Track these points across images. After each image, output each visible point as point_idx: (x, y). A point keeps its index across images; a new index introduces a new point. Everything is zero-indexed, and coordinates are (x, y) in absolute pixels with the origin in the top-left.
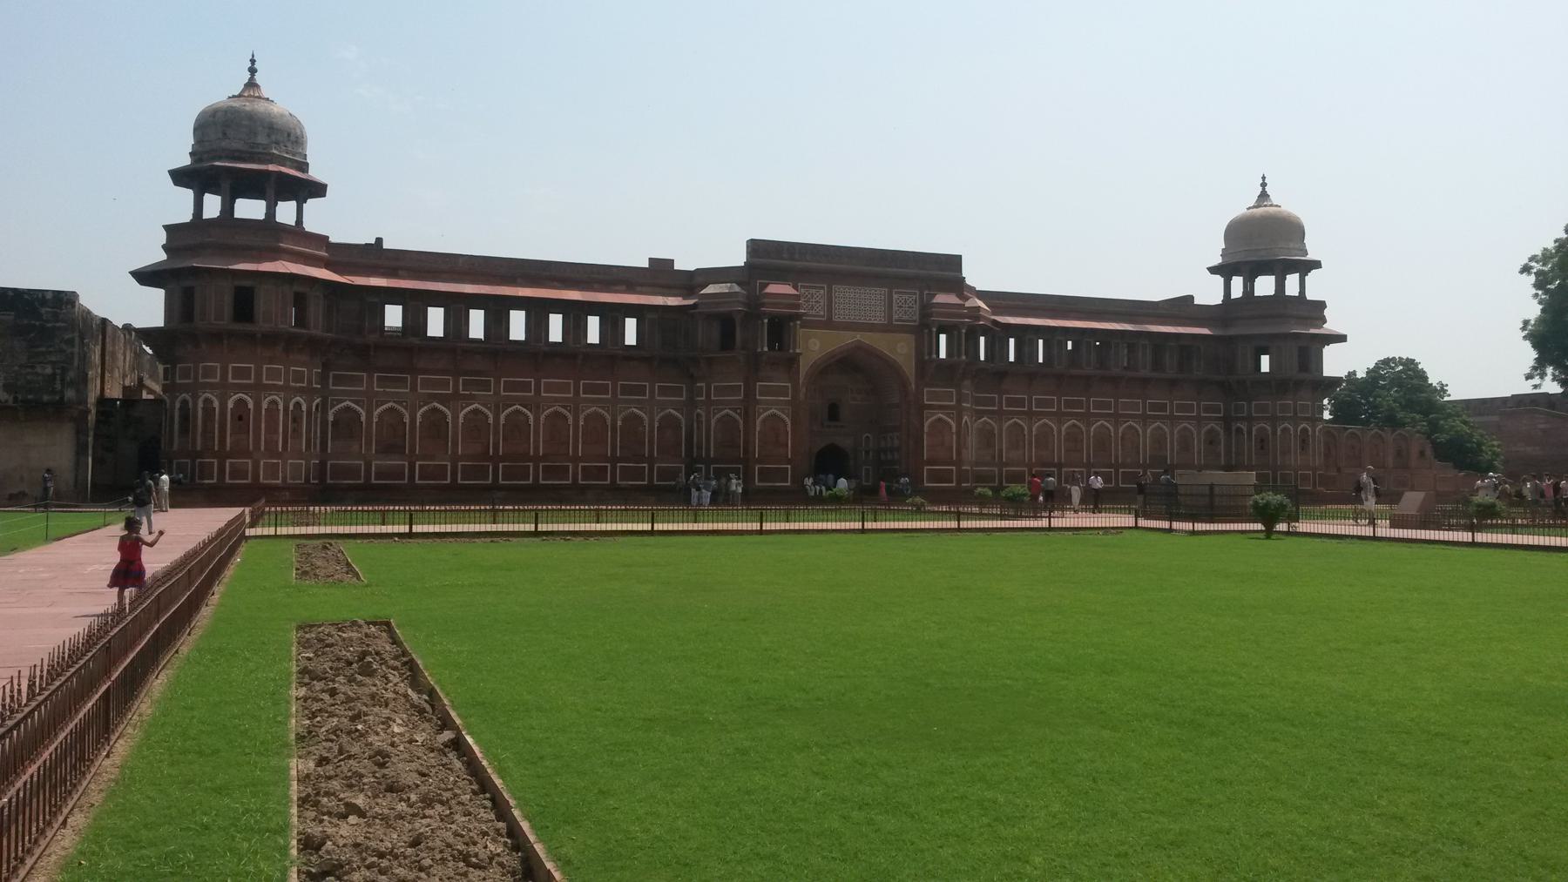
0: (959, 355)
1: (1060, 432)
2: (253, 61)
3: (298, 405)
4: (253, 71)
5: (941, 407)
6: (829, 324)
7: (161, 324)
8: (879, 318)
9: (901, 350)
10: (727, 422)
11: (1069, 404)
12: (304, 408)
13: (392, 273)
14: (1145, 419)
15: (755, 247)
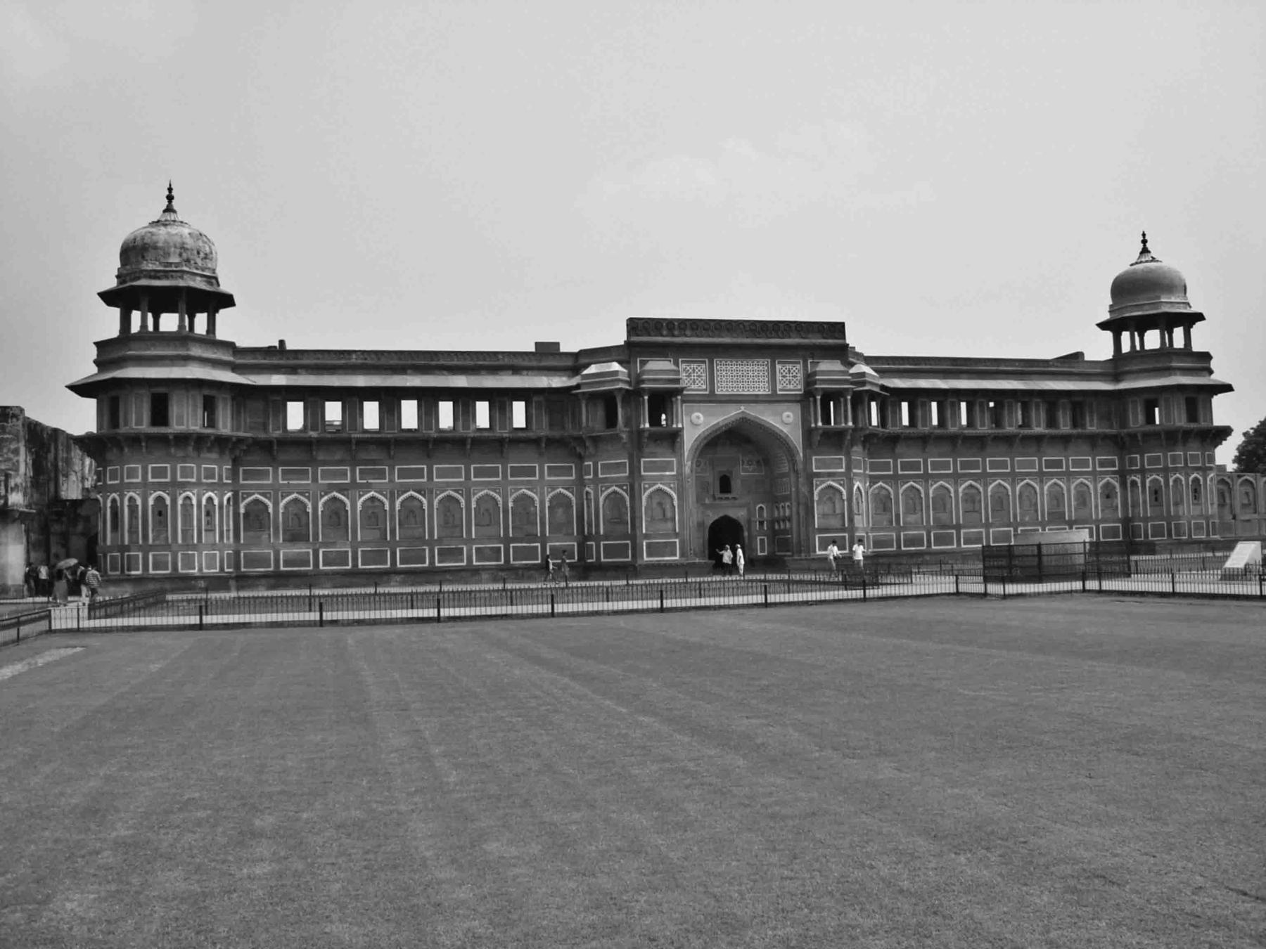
0: (846, 422)
1: (956, 492)
2: (170, 190)
3: (210, 499)
4: (170, 198)
5: (830, 475)
6: (711, 398)
7: (93, 428)
8: (763, 389)
9: (785, 422)
10: (615, 499)
11: (965, 465)
12: (216, 502)
13: (293, 370)
14: (1041, 477)
15: (634, 325)
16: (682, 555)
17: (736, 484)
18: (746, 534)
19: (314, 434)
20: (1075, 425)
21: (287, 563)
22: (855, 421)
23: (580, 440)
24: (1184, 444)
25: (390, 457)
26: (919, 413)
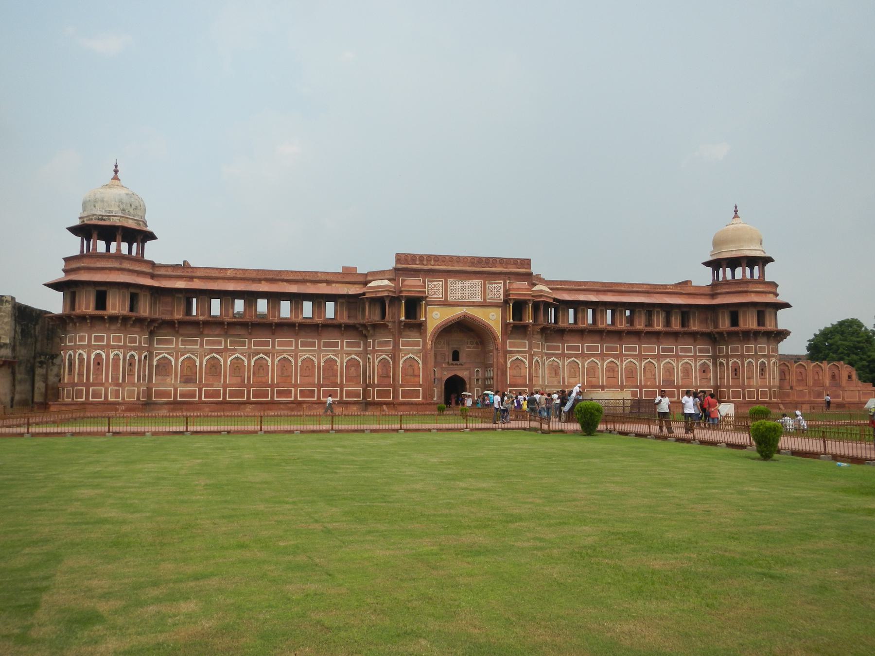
2: (116, 166)
3: (132, 356)
4: (116, 172)
5: (518, 352)
6: (445, 303)
8: (478, 299)
9: (492, 318)
10: (384, 362)
11: (608, 349)
12: (137, 358)
13: (191, 278)
14: (659, 357)
15: (399, 258)
16: (423, 398)
17: (463, 357)
18: (468, 386)
19: (201, 318)
20: (683, 325)
21: (182, 396)
22: (535, 318)
23: (364, 325)
24: (756, 339)
25: (250, 334)
26: (580, 315)
